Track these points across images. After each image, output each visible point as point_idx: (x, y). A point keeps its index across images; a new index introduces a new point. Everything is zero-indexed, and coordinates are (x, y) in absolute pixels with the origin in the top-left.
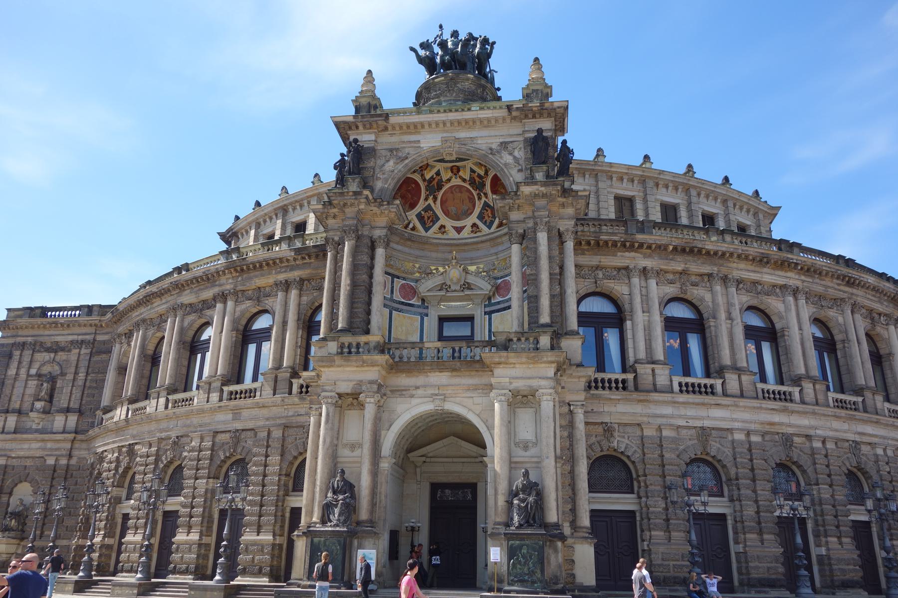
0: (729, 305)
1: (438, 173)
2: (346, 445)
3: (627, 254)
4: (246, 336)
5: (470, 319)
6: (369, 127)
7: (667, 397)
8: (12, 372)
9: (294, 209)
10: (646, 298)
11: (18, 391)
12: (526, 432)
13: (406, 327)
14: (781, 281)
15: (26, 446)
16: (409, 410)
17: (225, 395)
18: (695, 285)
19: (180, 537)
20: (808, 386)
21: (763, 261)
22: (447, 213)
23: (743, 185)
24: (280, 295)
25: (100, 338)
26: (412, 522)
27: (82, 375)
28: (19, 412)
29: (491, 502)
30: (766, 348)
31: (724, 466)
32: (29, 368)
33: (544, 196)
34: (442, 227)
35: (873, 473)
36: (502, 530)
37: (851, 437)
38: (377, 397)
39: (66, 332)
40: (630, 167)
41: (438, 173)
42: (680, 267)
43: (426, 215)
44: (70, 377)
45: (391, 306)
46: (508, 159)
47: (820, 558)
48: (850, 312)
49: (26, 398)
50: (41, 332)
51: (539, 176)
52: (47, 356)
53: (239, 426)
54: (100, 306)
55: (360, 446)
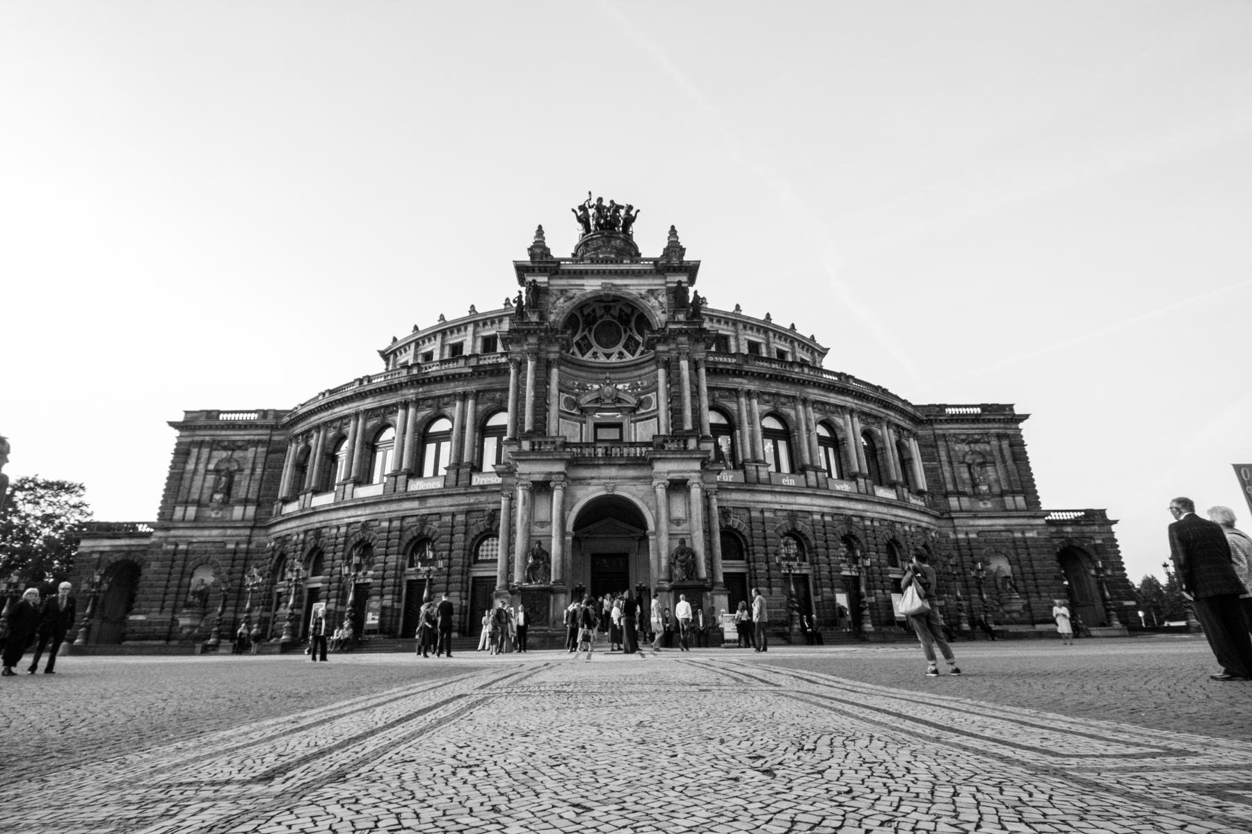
0: (808, 420)
1: (594, 311)
2: (536, 524)
3: (736, 380)
4: (423, 437)
5: (619, 426)
6: (543, 271)
7: (768, 488)
8: (190, 466)
9: (452, 332)
10: (750, 413)
12: (679, 512)
13: (572, 431)
15: (206, 533)
16: (586, 495)
18: (783, 404)
20: (861, 481)
21: (829, 387)
22: (599, 342)
23: (804, 331)
24: (458, 404)
25: (275, 438)
26: (579, 583)
27: (259, 471)
28: (199, 504)
29: (653, 563)
30: (831, 450)
31: (807, 539)
32: (208, 461)
33: (686, 333)
34: (595, 354)
35: (903, 543)
36: (667, 585)
37: (889, 517)
38: (564, 484)
40: (726, 313)
41: (594, 311)
42: (774, 391)
43: (582, 343)
44: (247, 472)
45: (563, 415)
46: (654, 302)
49: (205, 491)
50: (218, 432)
51: (681, 317)
52: (224, 454)
54: (275, 411)
55: (550, 523)
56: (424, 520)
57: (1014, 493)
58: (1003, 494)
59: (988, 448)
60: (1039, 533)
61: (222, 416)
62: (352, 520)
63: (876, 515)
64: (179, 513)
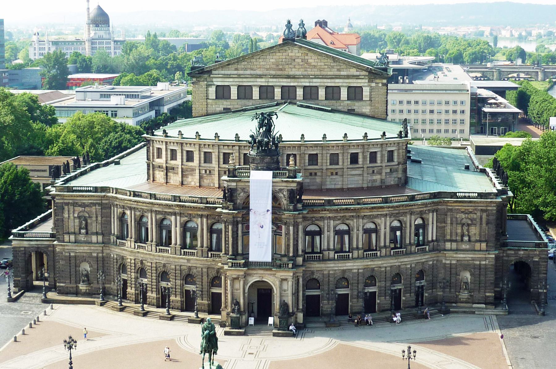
3: (323, 212)
8: (66, 215)
10: (329, 227)
11: (71, 224)
14: (380, 213)
15: (82, 248)
16: (252, 280)
17: (182, 253)
18: (348, 219)
19: (172, 298)
20: (384, 251)
25: (103, 202)
27: (99, 218)
28: (74, 233)
37: (397, 264)
39: (87, 198)
42: (342, 215)
44: (94, 219)
47: (378, 303)
48: (408, 216)
49: (76, 227)
50: (75, 198)
51: (291, 207)
52: (81, 209)
53: (190, 265)
56: (190, 268)
57: (480, 241)
58: (477, 241)
59: (475, 216)
60: (489, 262)
61: (74, 188)
62: (158, 261)
63: (389, 265)
64: (66, 238)
